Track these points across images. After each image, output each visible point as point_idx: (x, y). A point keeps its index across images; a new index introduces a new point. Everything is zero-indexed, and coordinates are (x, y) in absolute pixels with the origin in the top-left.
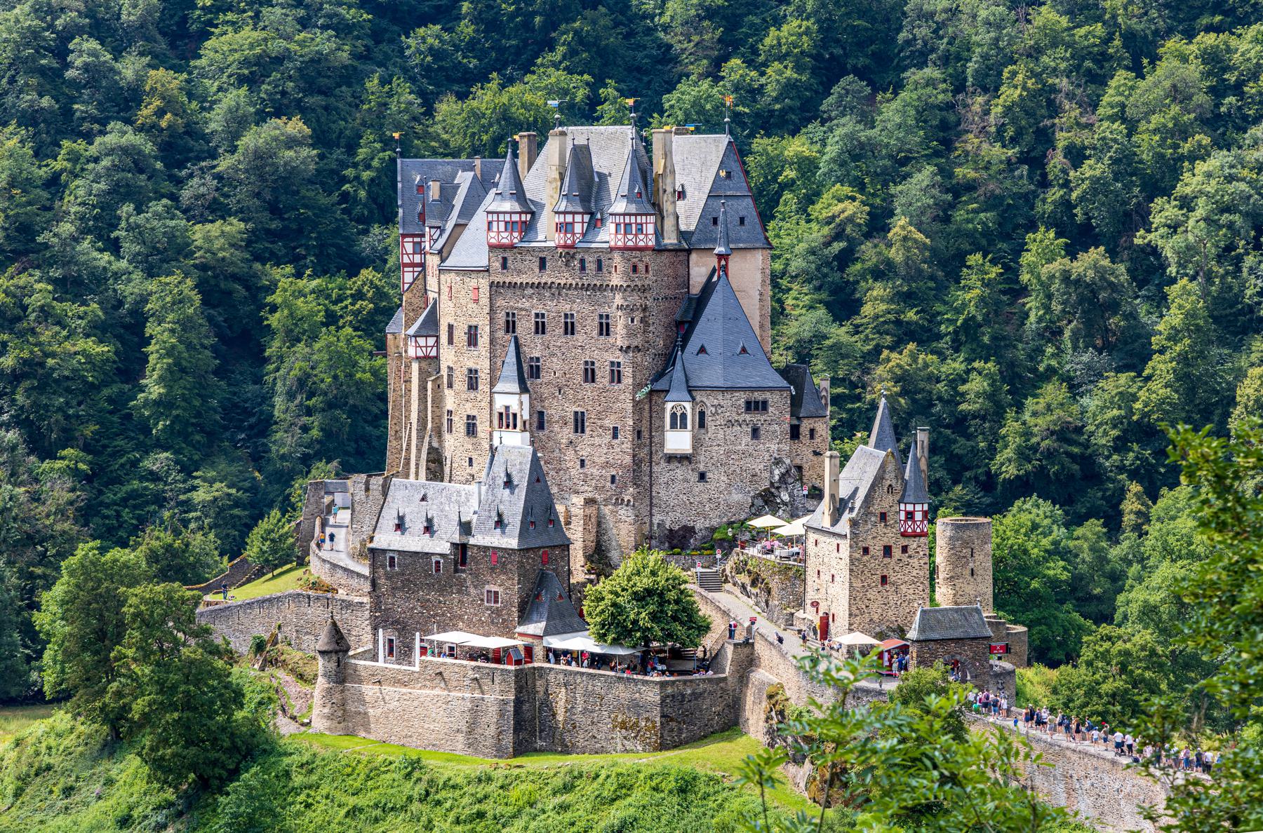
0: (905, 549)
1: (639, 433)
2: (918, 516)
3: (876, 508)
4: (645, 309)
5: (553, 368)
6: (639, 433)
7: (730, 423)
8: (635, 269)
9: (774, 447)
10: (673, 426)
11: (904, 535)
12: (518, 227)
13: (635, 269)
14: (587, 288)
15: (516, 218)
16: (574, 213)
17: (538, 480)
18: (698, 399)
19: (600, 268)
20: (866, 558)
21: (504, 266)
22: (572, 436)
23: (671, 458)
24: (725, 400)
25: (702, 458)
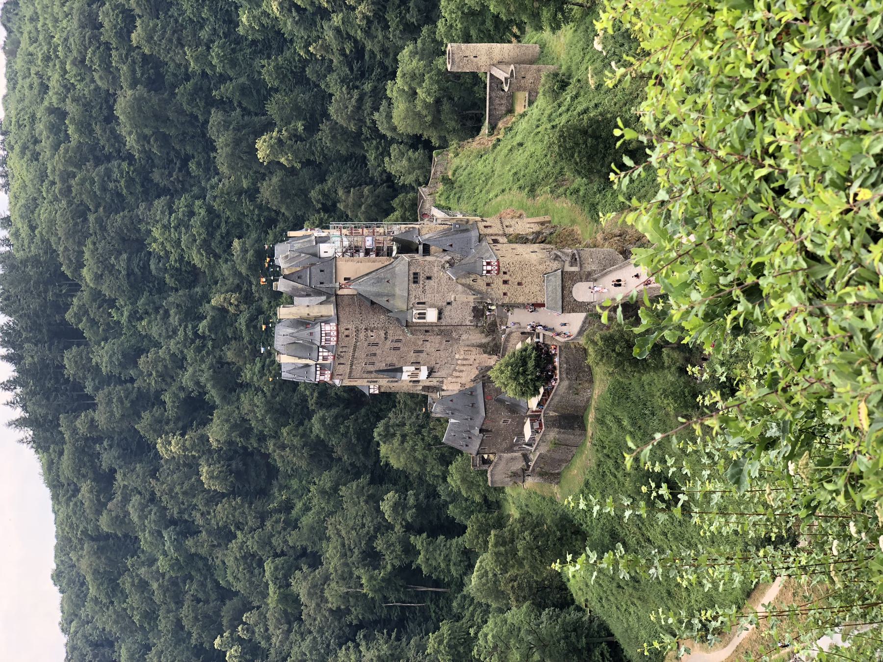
0: (505, 273)
1: (427, 331)
2: (489, 268)
3: (484, 288)
5: (393, 359)
6: (427, 331)
7: (424, 292)
8: (347, 336)
9: (436, 269)
10: (424, 318)
11: (498, 274)
13: (347, 336)
14: (354, 350)
15: (318, 373)
22: (425, 354)
23: (439, 318)
24: (413, 293)
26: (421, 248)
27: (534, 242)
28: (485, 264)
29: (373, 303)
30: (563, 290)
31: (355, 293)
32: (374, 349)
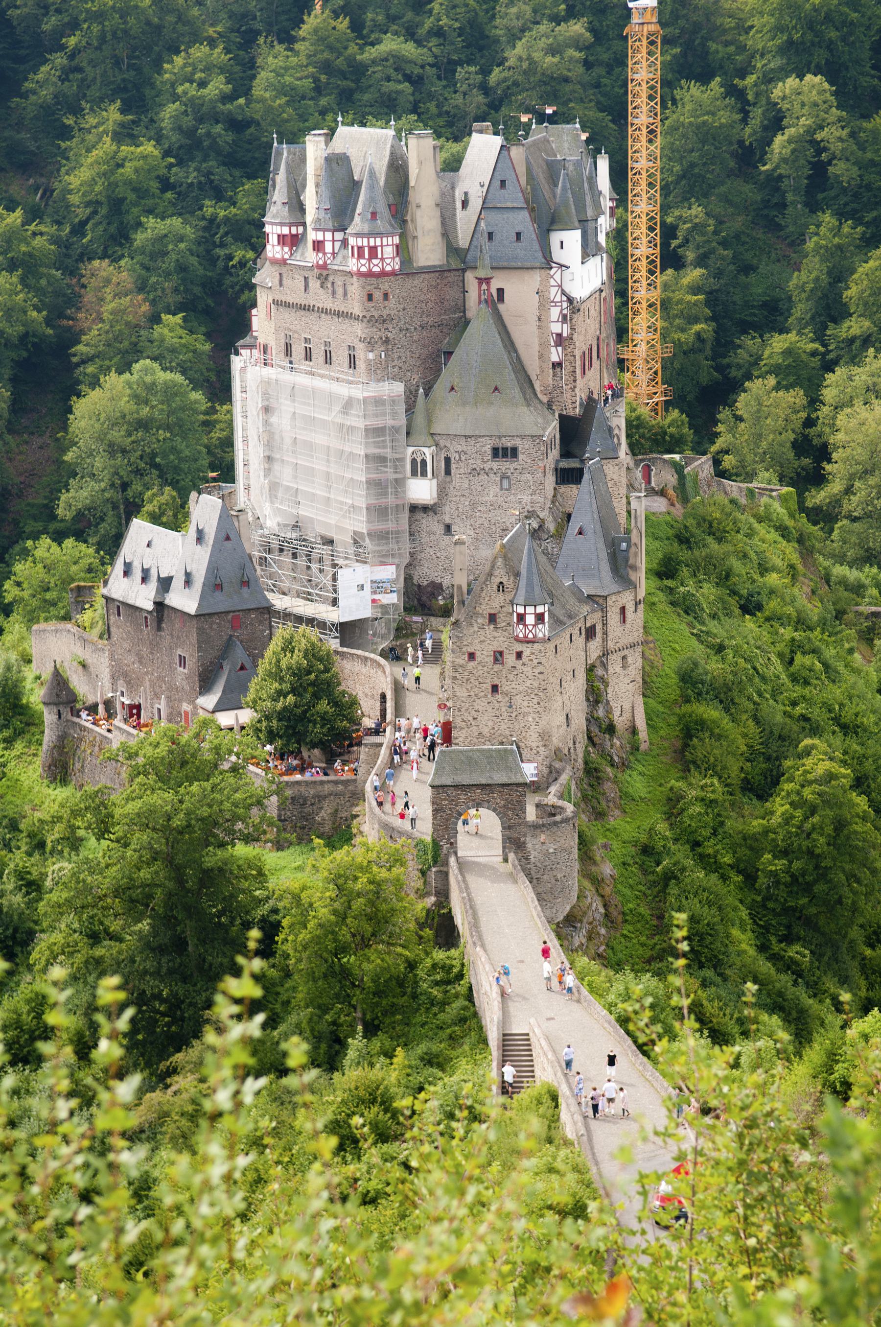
0: (519, 655)
2: (530, 620)
3: (485, 609)
4: (387, 341)
7: (475, 472)
9: (526, 498)
10: (414, 473)
12: (288, 240)
13: (370, 297)
14: (338, 314)
15: (285, 230)
16: (324, 230)
17: (228, 538)
18: (442, 444)
19: (345, 294)
20: (472, 664)
21: (281, 285)
24: (470, 447)
25: (447, 509)
26: (574, 464)
27: (591, 719)
28: (540, 609)
29: (449, 354)
30: (483, 787)
31: (469, 314)
32: (341, 357)
